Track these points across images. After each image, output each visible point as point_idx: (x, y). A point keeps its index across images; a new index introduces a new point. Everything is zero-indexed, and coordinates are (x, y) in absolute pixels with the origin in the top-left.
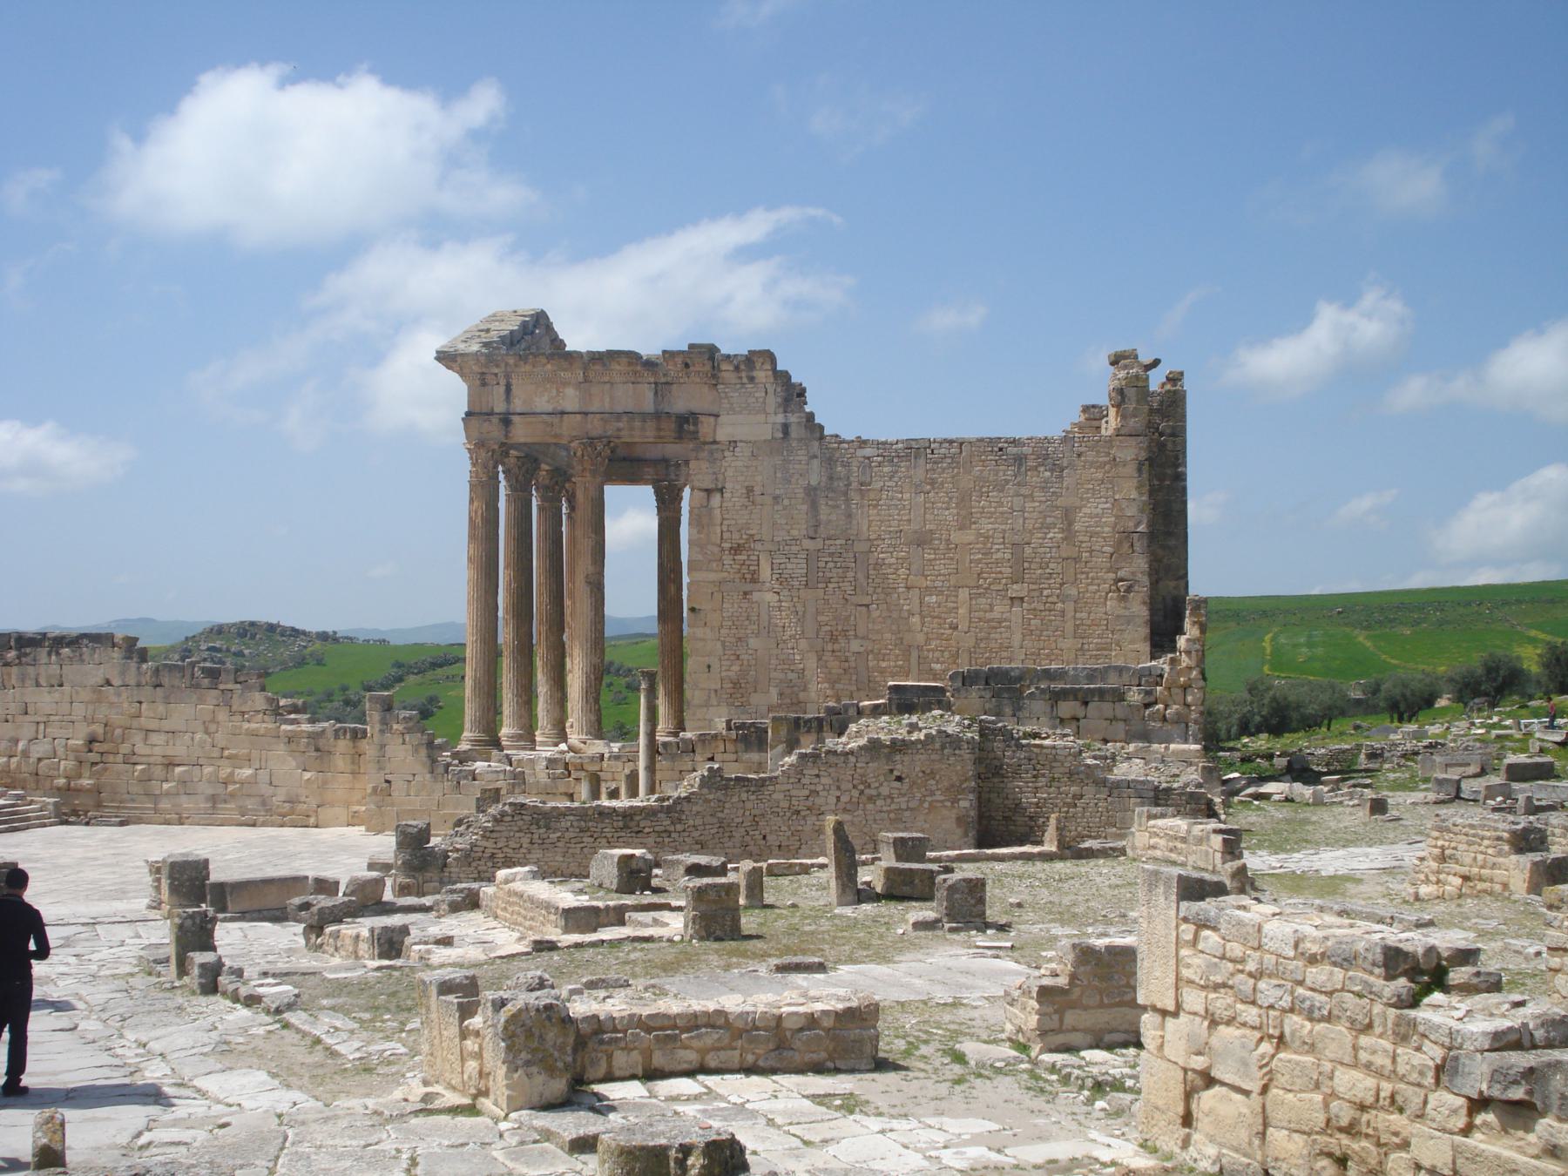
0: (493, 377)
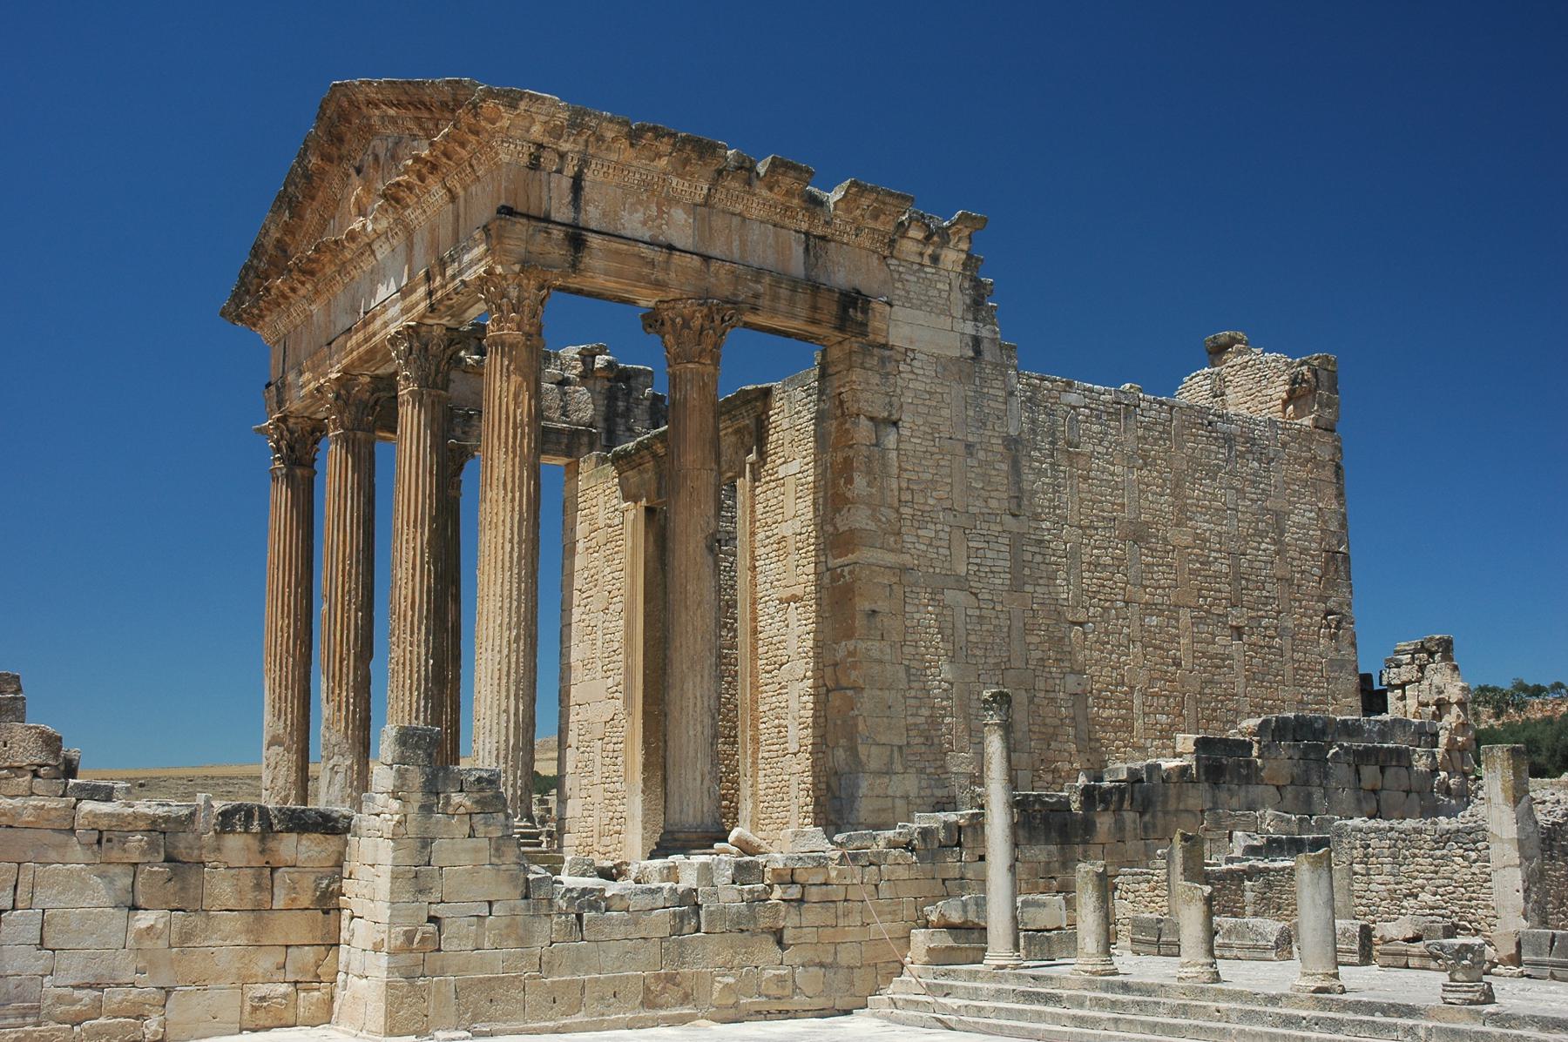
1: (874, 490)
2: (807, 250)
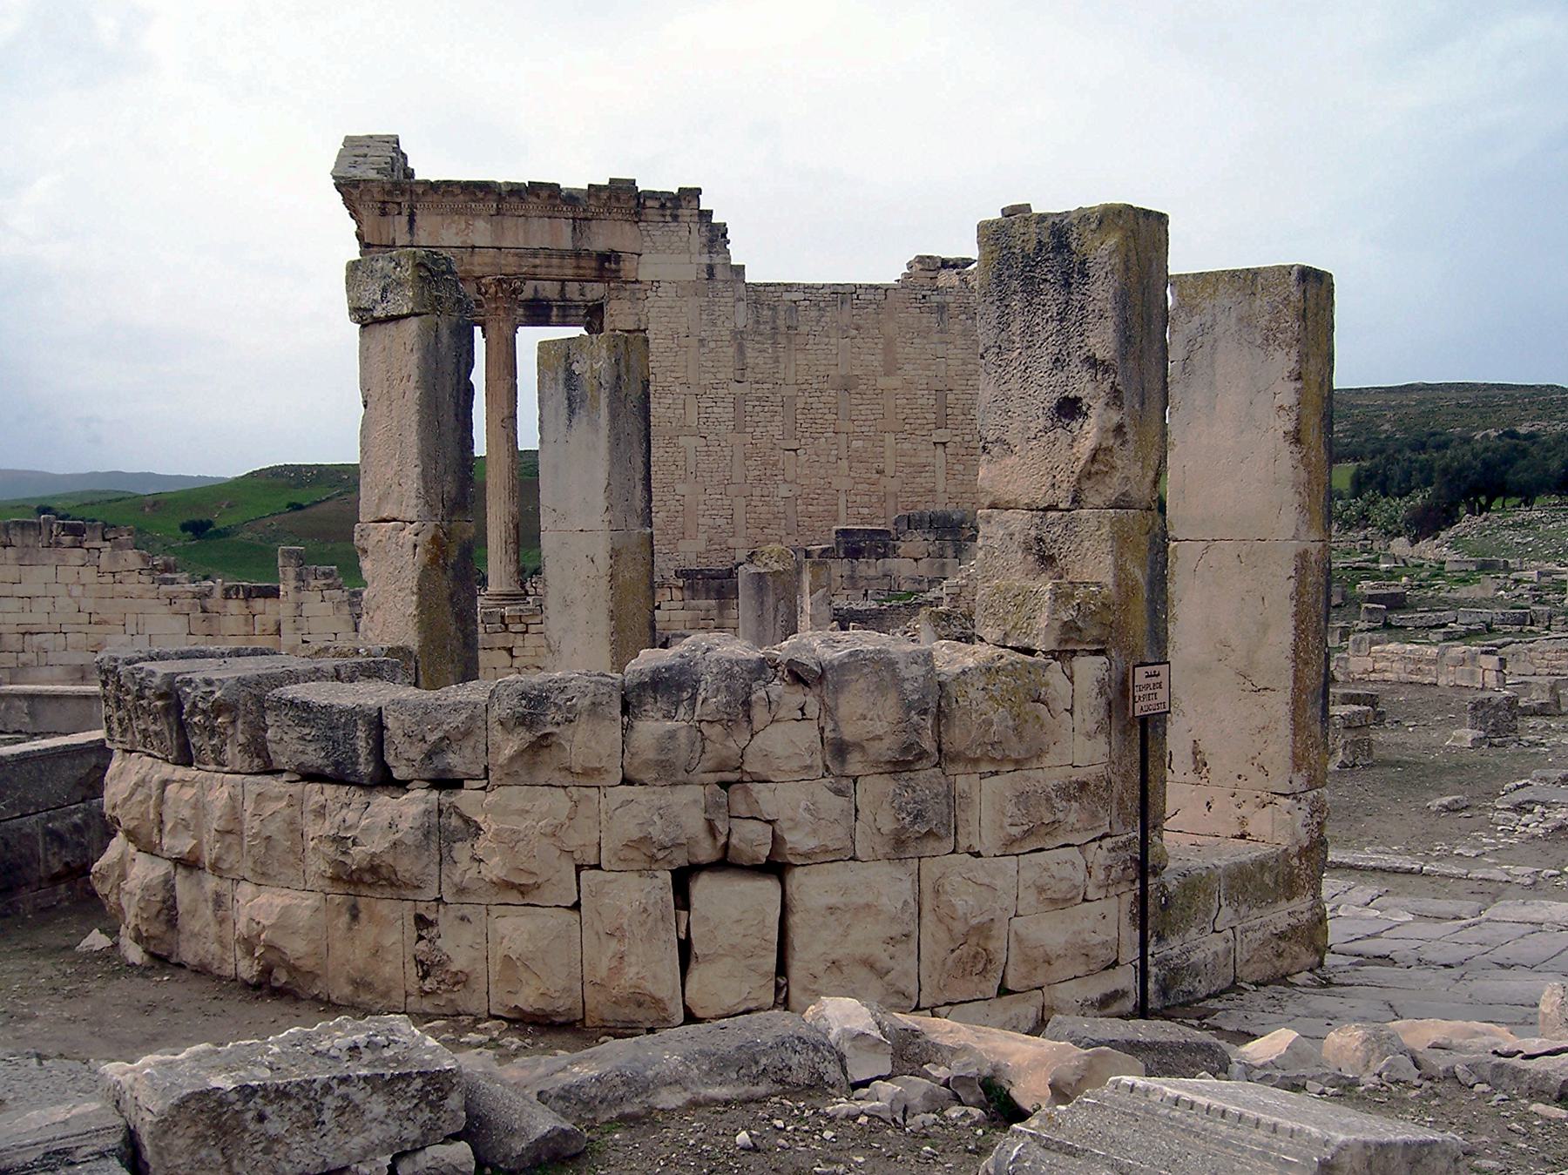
0: (395, 206)
2: (574, 228)
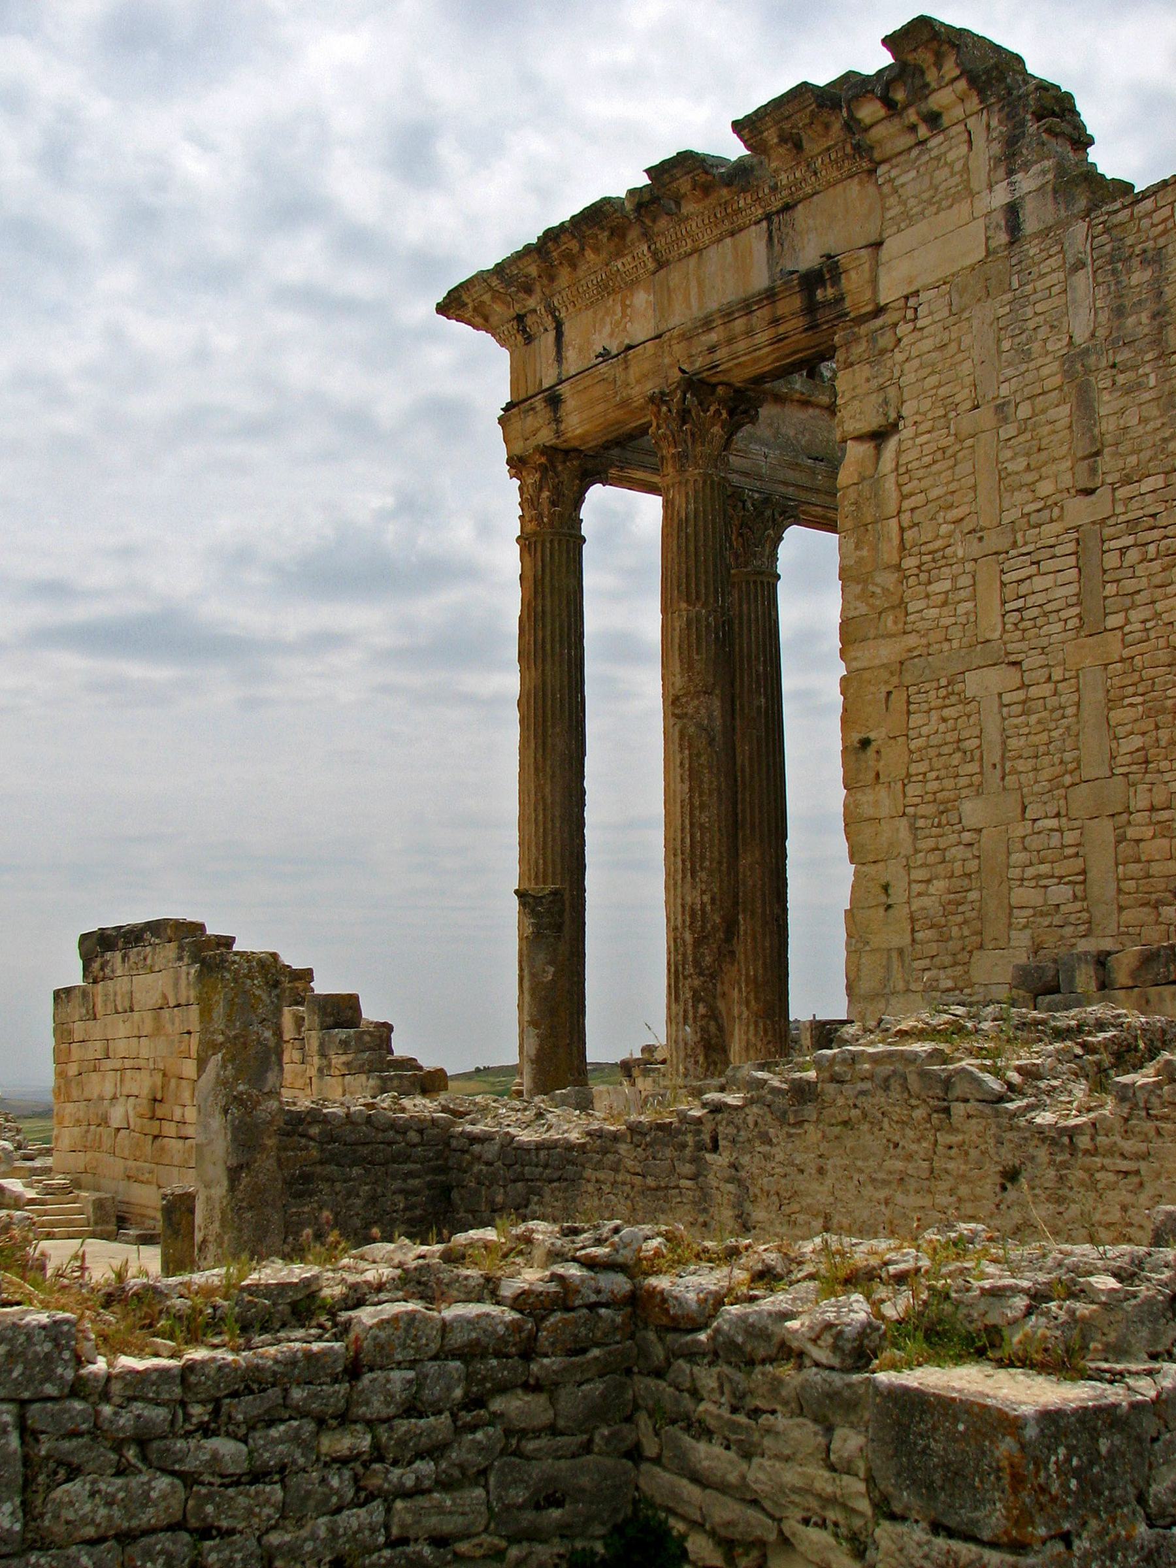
1: (865, 553)
2: (770, 238)
